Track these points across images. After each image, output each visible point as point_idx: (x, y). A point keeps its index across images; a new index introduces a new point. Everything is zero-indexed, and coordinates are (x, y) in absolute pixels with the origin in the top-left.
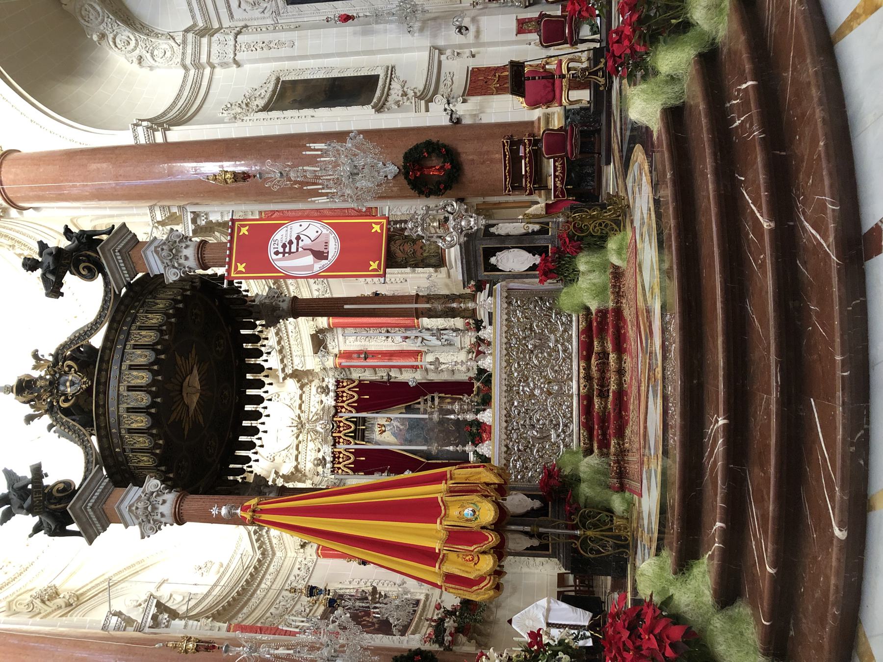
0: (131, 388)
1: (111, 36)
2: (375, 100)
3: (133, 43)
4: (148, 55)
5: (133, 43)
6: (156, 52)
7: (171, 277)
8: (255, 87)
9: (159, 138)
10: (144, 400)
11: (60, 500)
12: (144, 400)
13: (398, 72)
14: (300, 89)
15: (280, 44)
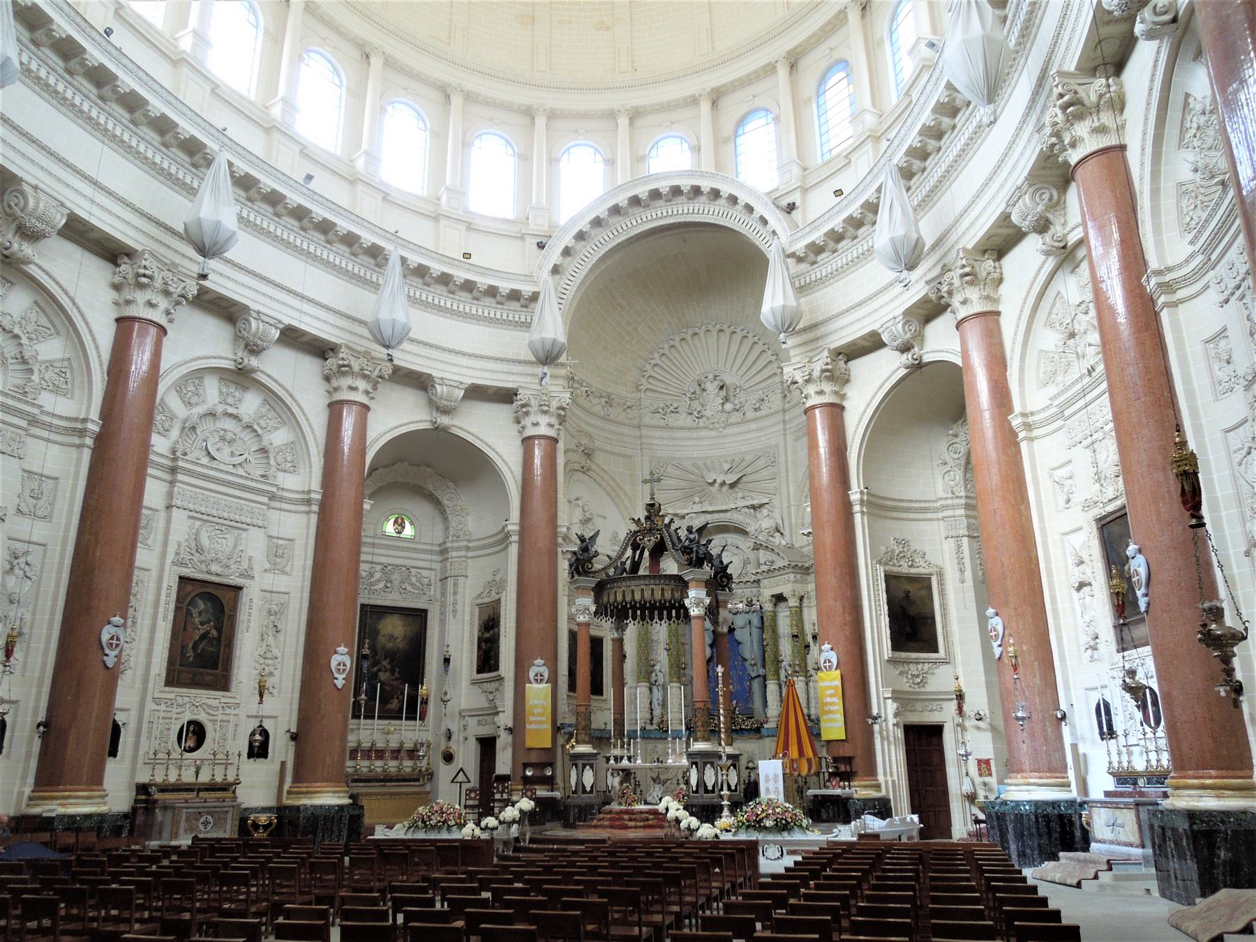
0: (633, 591)
1: (957, 440)
2: (904, 655)
3: (956, 456)
4: (949, 468)
5: (956, 456)
6: (952, 473)
7: (687, 602)
8: (927, 557)
9: (857, 508)
10: (628, 598)
11: (583, 568)
12: (628, 598)
13: (943, 669)
14: (923, 593)
15: (962, 571)
